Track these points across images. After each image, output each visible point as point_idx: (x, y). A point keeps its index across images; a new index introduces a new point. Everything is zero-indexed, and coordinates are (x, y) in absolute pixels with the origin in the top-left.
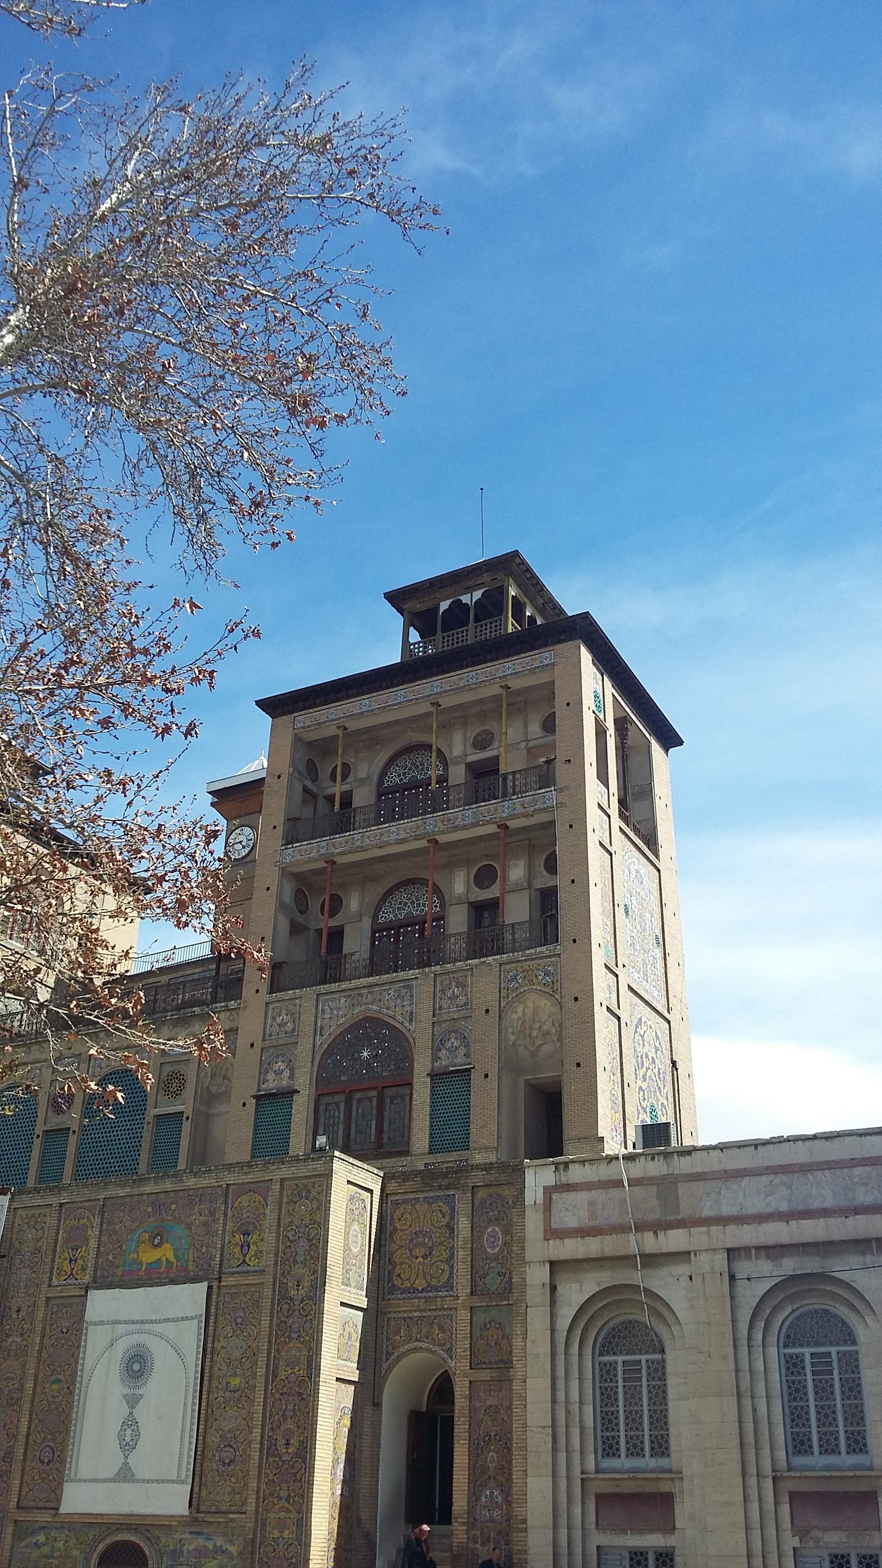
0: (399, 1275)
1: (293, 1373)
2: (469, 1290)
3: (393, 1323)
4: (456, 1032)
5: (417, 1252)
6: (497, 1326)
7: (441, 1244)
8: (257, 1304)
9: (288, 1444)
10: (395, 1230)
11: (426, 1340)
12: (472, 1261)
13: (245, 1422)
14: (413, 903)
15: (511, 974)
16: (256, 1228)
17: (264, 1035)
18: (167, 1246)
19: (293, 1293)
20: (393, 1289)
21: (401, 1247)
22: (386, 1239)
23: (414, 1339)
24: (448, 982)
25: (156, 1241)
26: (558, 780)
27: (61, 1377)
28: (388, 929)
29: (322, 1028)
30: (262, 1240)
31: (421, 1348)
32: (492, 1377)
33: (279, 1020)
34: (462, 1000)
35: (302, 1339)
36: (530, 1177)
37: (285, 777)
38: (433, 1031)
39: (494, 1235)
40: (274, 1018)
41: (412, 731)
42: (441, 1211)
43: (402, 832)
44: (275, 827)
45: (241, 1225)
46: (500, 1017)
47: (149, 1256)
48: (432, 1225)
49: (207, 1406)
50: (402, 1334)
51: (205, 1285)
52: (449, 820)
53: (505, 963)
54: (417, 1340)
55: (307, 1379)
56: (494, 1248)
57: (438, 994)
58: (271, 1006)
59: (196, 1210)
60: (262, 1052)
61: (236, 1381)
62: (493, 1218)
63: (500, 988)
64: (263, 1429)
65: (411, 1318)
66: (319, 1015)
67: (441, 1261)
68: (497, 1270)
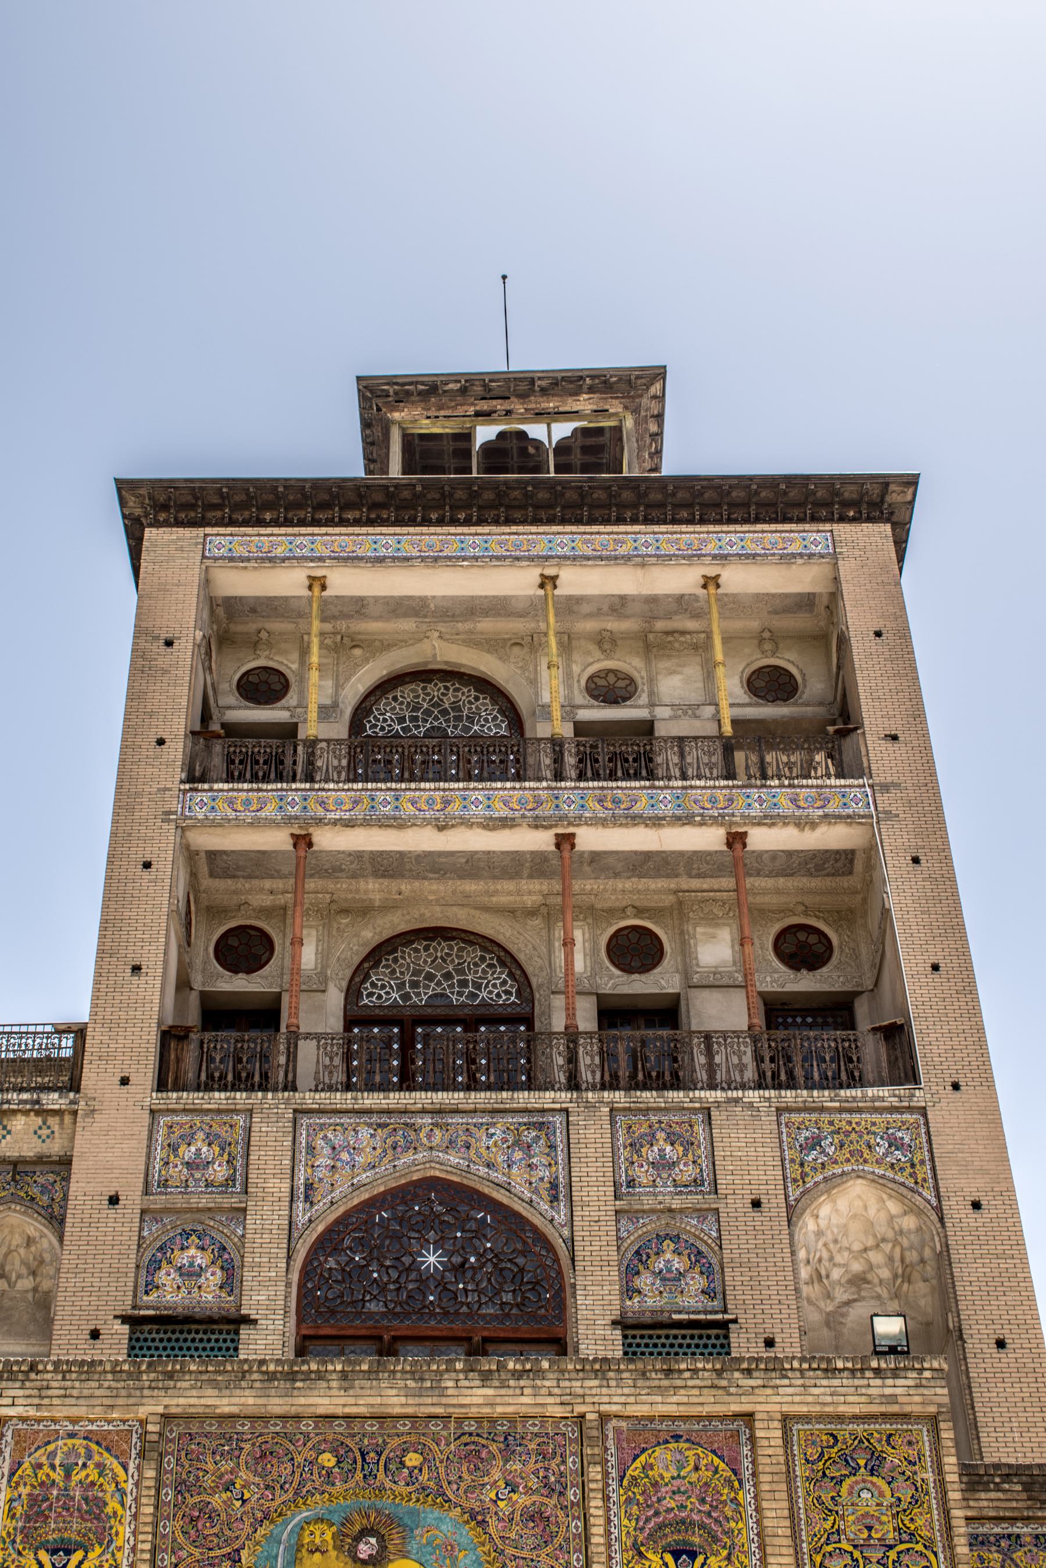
4: (676, 1239)
14: (448, 976)
16: (716, 1539)
17: (147, 1183)
24: (645, 1129)
28: (384, 1022)
29: (309, 1187)
33: (188, 1153)
34: (686, 1172)
40: (174, 1148)
41: (440, 637)
43: (497, 804)
45: (661, 1527)
46: (789, 1221)
52: (616, 801)
53: (789, 1110)
58: (163, 1120)
59: (496, 1474)
60: (142, 1220)
63: (783, 1160)
66: (302, 1156)
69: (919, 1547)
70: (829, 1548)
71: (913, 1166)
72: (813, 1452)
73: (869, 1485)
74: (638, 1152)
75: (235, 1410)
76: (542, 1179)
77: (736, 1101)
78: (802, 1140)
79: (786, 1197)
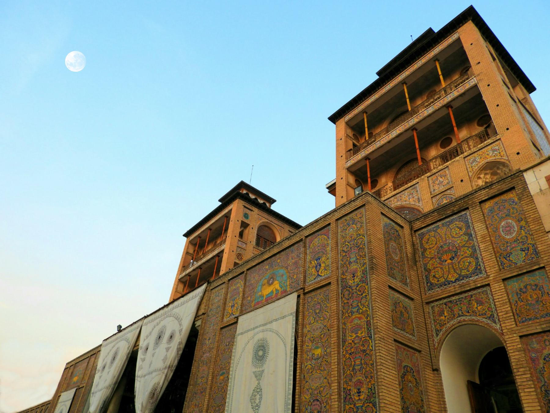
0: (434, 276)
1: (358, 337)
2: (497, 268)
3: (436, 309)
5: (445, 257)
6: (534, 287)
7: (464, 246)
8: (327, 299)
9: (359, 392)
10: (425, 250)
11: (467, 314)
12: (493, 248)
13: (326, 380)
15: (472, 160)
16: (324, 253)
18: (276, 282)
19: (351, 282)
20: (431, 286)
21: (431, 258)
22: (419, 257)
23: (456, 316)
24: (436, 178)
25: (271, 282)
26: (475, 72)
27: (224, 371)
30: (328, 259)
31: (464, 321)
32: (542, 328)
35: (361, 311)
36: (529, 177)
37: (343, 138)
38: (432, 202)
39: (509, 226)
42: (457, 227)
44: (342, 156)
46: (471, 181)
47: (267, 291)
48: (453, 237)
49: (301, 373)
50: (446, 314)
51: (295, 295)
54: (458, 317)
55: (368, 338)
56: (513, 233)
57: (431, 185)
61: (318, 352)
62: (504, 215)
63: (467, 168)
64: (339, 383)
65: (451, 301)
67: (466, 257)
68: (519, 248)
69: (361, 237)
70: (344, 245)
71: (500, 153)
72: (342, 226)
73: (352, 228)
74: (435, 183)
75: (255, 264)
76: (416, 199)
77: (454, 161)
78: (471, 162)
79: (469, 176)
